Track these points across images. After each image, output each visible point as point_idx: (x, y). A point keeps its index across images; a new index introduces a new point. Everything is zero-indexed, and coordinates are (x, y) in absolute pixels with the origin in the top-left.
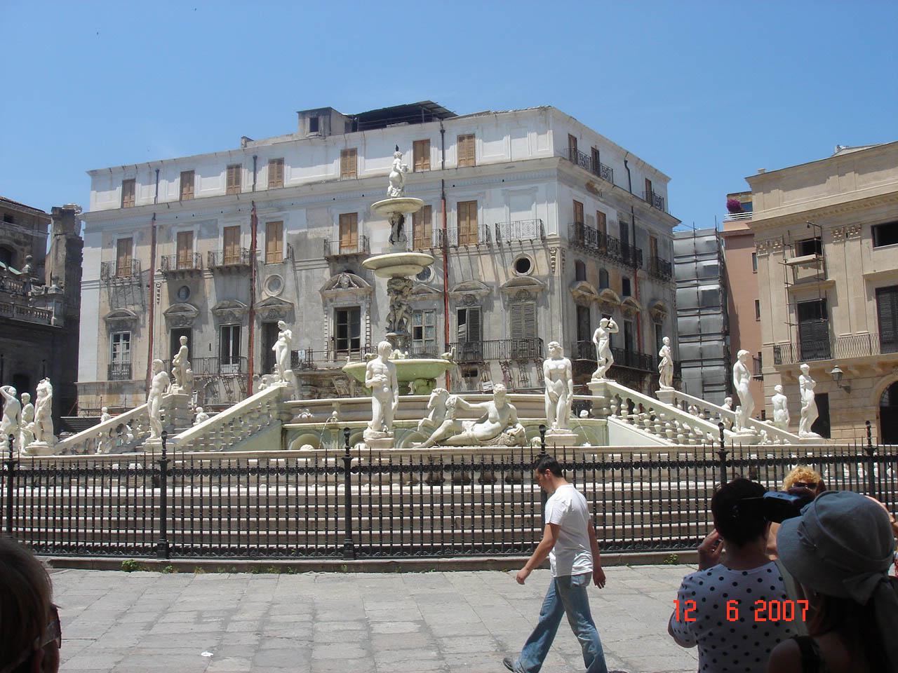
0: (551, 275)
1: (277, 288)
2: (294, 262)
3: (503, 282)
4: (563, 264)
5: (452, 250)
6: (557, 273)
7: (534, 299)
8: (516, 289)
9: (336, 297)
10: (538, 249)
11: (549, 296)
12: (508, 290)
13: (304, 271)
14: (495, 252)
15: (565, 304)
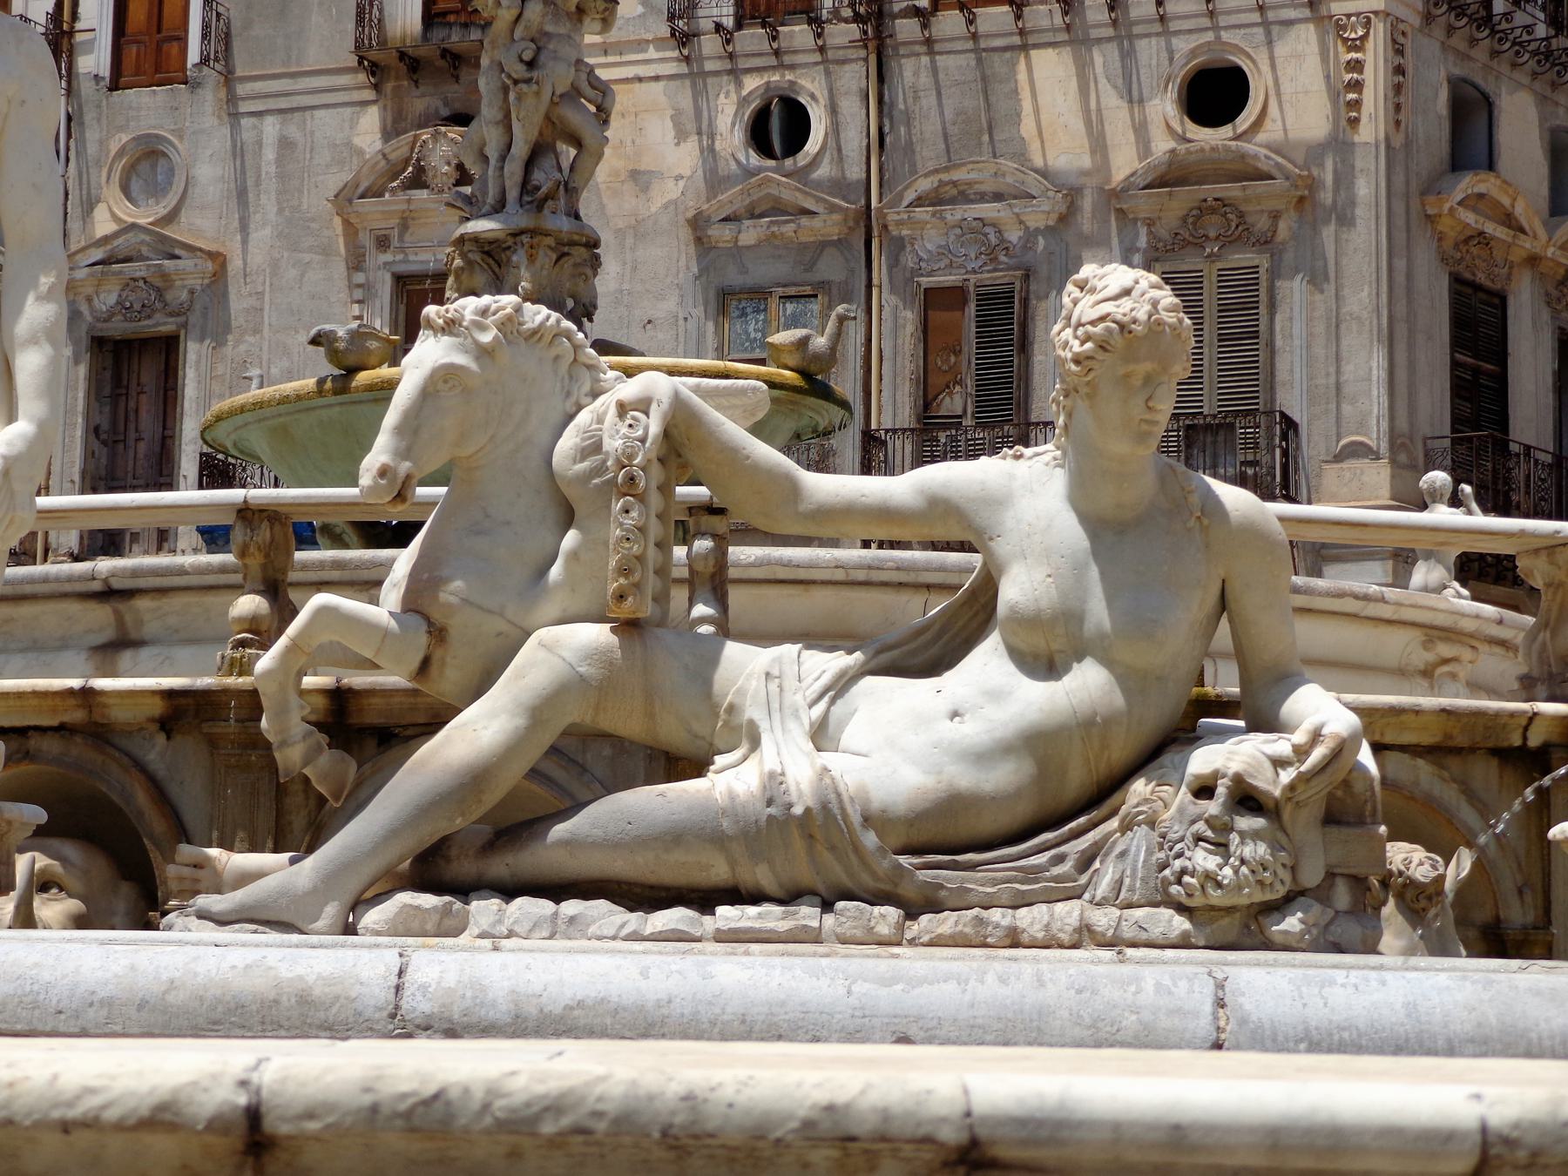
0: (1339, 144)
1: (157, 191)
2: (229, 78)
3: (1124, 163)
4: (1398, 89)
5: (907, 29)
6: (1371, 129)
7: (1266, 242)
8: (1183, 199)
9: (404, 226)
10: (1289, 23)
11: (1328, 233)
12: (1144, 204)
13: (269, 120)
14: (1094, 33)
15: (1400, 264)
